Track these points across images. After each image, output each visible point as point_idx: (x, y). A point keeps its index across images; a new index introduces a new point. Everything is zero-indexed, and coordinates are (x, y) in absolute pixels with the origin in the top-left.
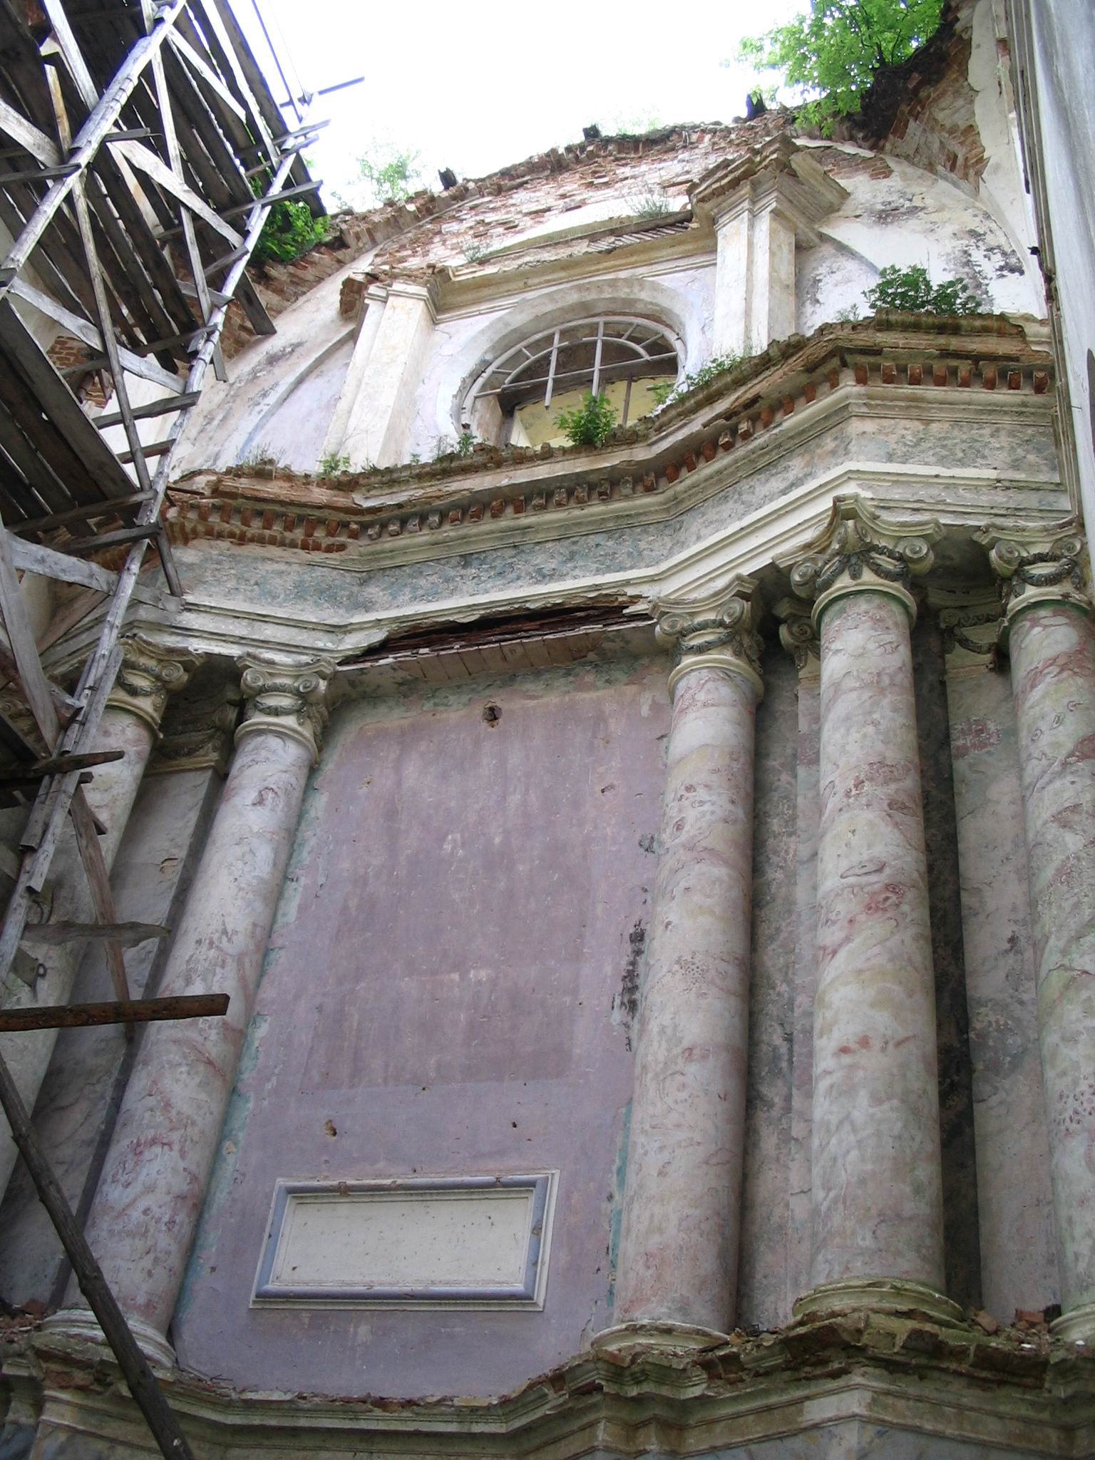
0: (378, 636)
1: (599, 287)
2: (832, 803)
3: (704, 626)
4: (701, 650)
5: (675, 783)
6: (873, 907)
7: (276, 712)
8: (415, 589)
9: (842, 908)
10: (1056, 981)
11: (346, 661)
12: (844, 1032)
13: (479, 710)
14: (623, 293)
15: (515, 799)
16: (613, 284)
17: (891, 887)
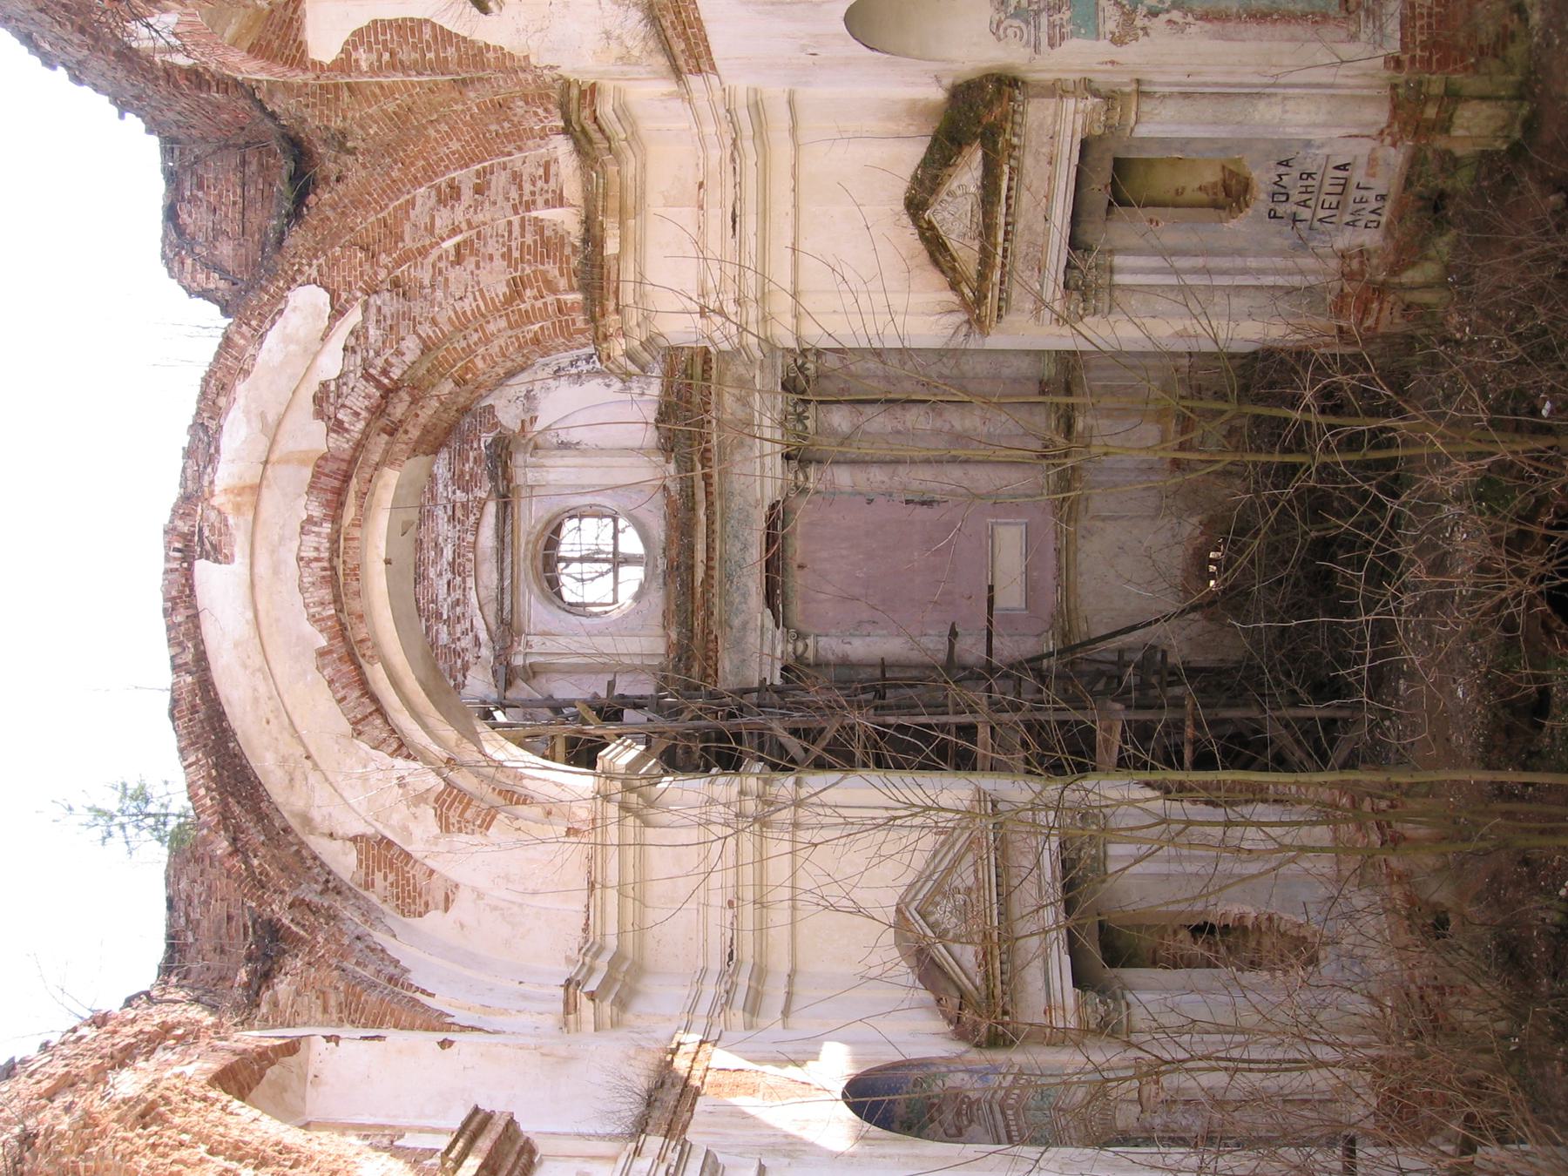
0: (768, 611)
1: (526, 550)
2: (900, 427)
3: (796, 478)
4: (807, 478)
5: (863, 486)
6: (941, 415)
7: (806, 646)
8: (740, 603)
9: (939, 423)
10: (955, 371)
11: (777, 626)
12: (978, 422)
13: (798, 573)
14: (532, 538)
15: (844, 552)
16: (527, 543)
17: (933, 410)
